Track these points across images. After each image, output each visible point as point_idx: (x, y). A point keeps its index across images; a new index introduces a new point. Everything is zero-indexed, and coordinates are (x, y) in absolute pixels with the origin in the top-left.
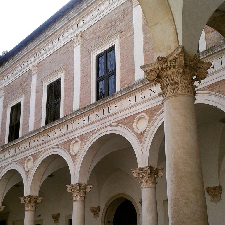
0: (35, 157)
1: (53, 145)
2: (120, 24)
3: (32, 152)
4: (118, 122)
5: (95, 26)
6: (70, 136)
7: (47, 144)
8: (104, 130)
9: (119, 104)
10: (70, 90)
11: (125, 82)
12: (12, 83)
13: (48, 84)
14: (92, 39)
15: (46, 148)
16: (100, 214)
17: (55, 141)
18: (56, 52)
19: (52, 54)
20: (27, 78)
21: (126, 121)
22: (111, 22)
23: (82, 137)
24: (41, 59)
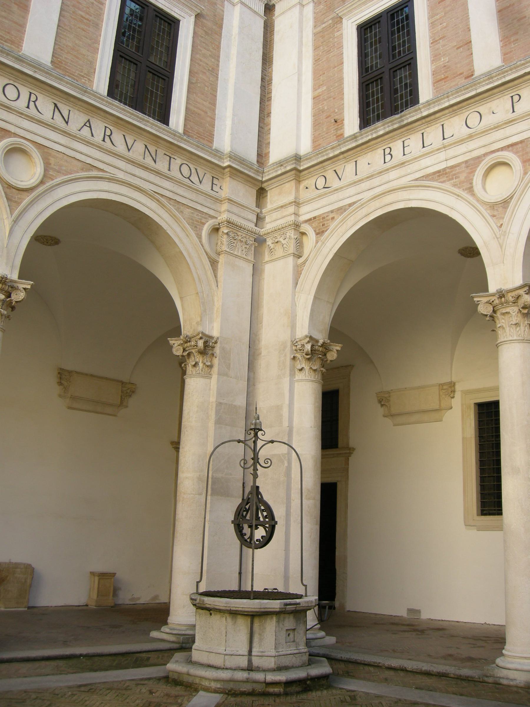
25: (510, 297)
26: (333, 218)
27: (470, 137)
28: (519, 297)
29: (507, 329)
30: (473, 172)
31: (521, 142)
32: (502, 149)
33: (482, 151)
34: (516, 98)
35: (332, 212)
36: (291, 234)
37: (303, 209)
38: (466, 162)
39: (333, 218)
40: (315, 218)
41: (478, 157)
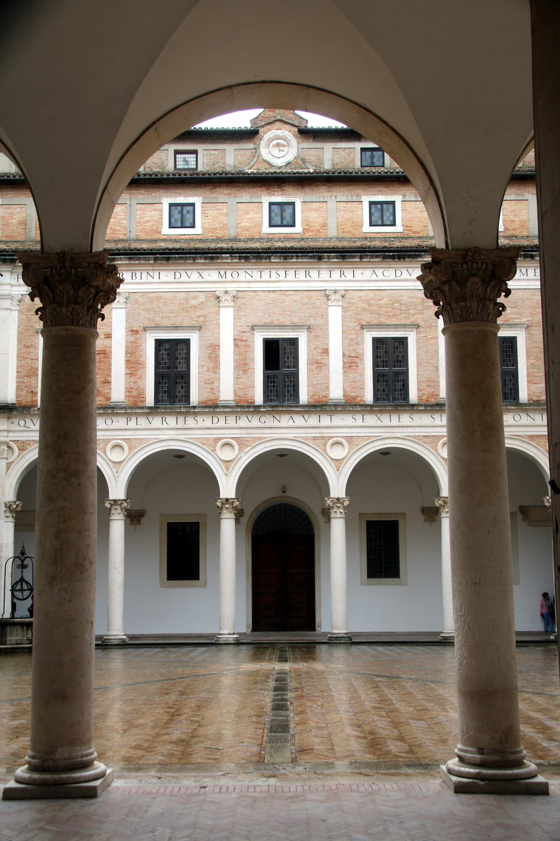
0: (242, 443)
1: (290, 436)
2: (415, 314)
3: (236, 433)
4: (414, 437)
5: (371, 294)
6: (326, 433)
7: (273, 431)
8: (391, 441)
9: (416, 417)
10: (320, 364)
11: (423, 392)
12: (155, 295)
13: (265, 337)
14: (365, 310)
15: (277, 436)
16: (244, 520)
17: (292, 431)
18: (283, 292)
19: (274, 291)
20: (203, 303)
21: (427, 440)
22: (401, 304)
23: (349, 439)
24: (243, 286)
25: (119, 502)
26: (29, 444)
27: (107, 430)
28: (122, 503)
29: (116, 514)
30: (106, 445)
31: (129, 439)
32: (120, 439)
33: (112, 437)
34: (129, 419)
35: (29, 441)
36: (6, 448)
37: (11, 434)
38: (104, 439)
39: (29, 444)
40: (18, 441)
41: (109, 439)
